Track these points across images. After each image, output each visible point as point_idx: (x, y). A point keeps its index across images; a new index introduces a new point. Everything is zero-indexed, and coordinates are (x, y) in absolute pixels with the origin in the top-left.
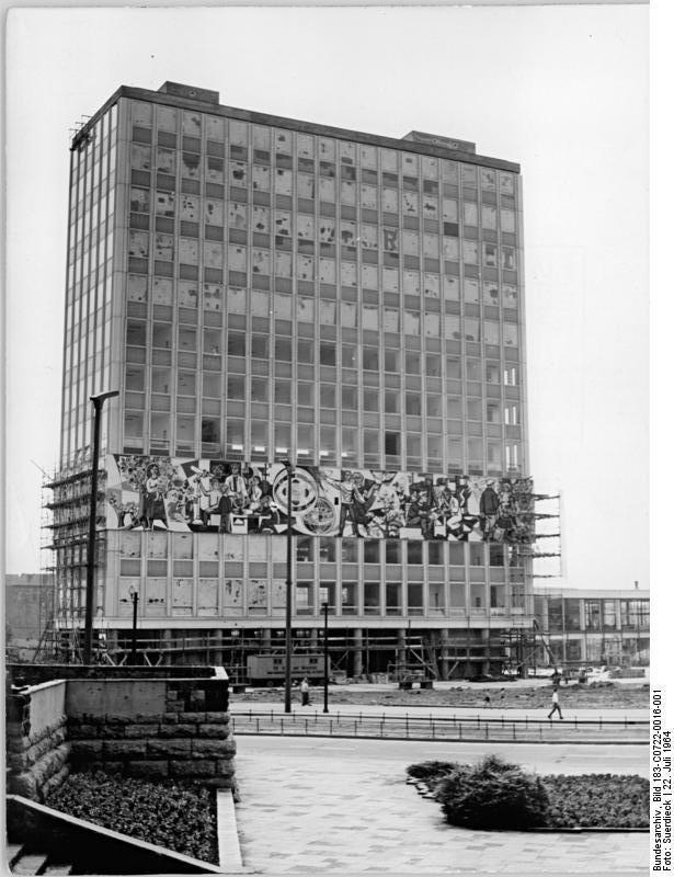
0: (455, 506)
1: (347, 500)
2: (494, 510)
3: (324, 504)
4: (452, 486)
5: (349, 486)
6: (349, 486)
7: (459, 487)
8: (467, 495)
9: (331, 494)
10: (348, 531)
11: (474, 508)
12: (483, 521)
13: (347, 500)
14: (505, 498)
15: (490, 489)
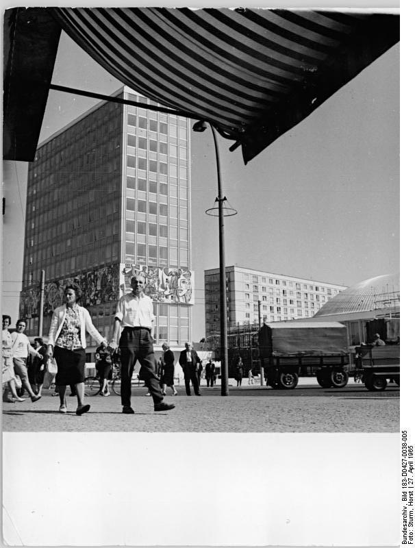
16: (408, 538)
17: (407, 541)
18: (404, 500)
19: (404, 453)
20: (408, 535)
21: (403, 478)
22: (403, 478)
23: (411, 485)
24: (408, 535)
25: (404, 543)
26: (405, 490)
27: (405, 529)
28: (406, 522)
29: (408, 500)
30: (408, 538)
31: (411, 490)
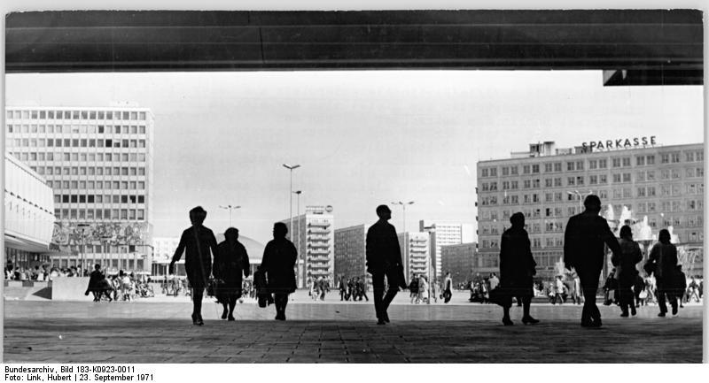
0: (114, 233)
1: (72, 233)
2: (131, 234)
3: (64, 234)
4: (113, 226)
5: (72, 228)
6: (72, 228)
7: (116, 226)
8: (120, 229)
9: (65, 230)
10: (72, 243)
11: (122, 233)
12: (126, 238)
13: (72, 233)
14: (136, 230)
15: (129, 227)
16: (13, 374)
17: (9, 373)
18: (63, 370)
19: (122, 369)
20: (17, 374)
21: (91, 368)
22: (91, 368)
23: (79, 377)
24: (17, 374)
25: (7, 369)
26: (75, 370)
27: (25, 370)
28: (35, 370)
29: (62, 375)
30: (13, 374)
31: (73, 378)
